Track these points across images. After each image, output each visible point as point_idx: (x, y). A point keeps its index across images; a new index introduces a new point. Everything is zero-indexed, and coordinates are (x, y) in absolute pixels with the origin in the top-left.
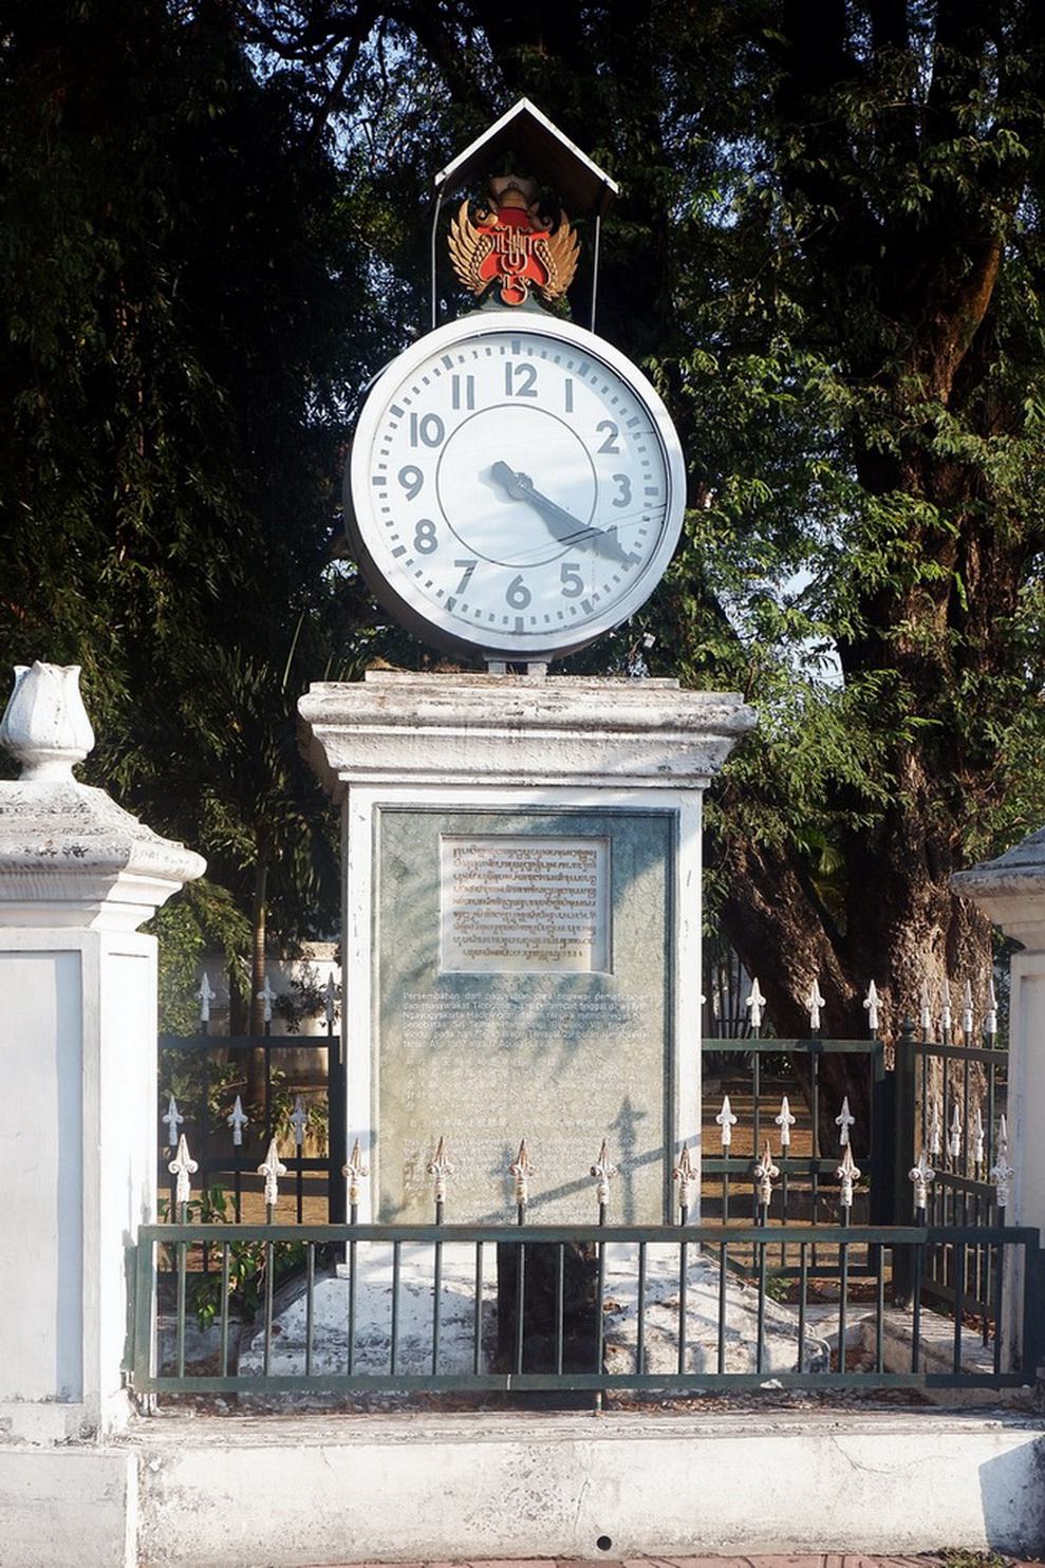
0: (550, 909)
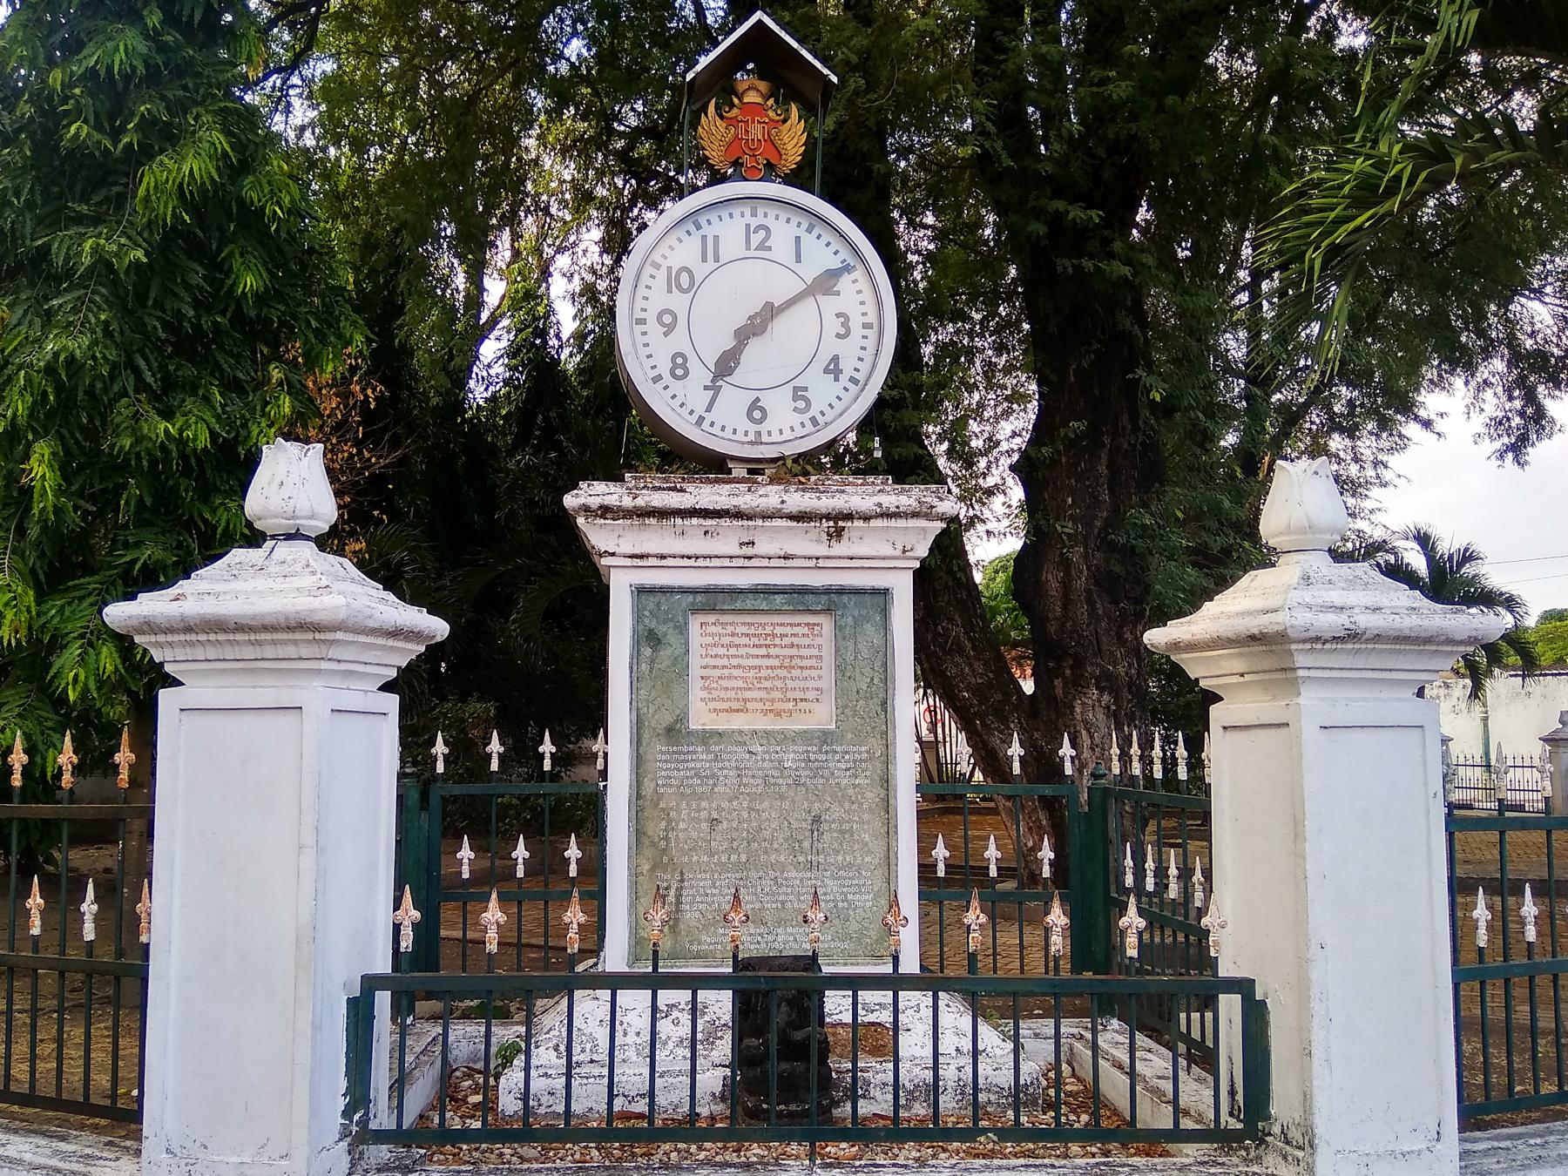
0: (783, 673)
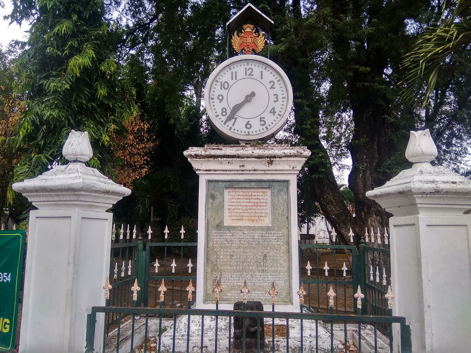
0: (254, 208)
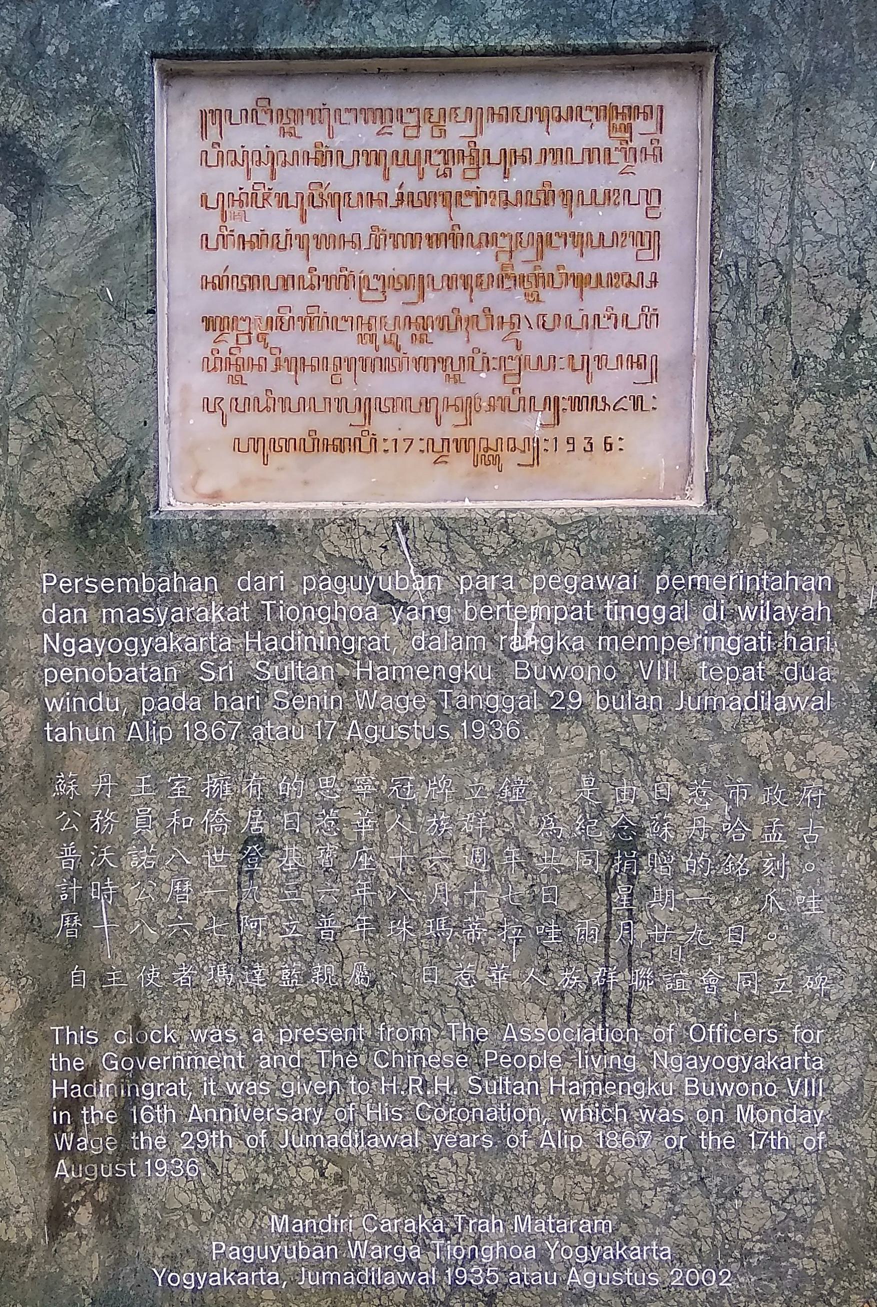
0: (509, 302)
